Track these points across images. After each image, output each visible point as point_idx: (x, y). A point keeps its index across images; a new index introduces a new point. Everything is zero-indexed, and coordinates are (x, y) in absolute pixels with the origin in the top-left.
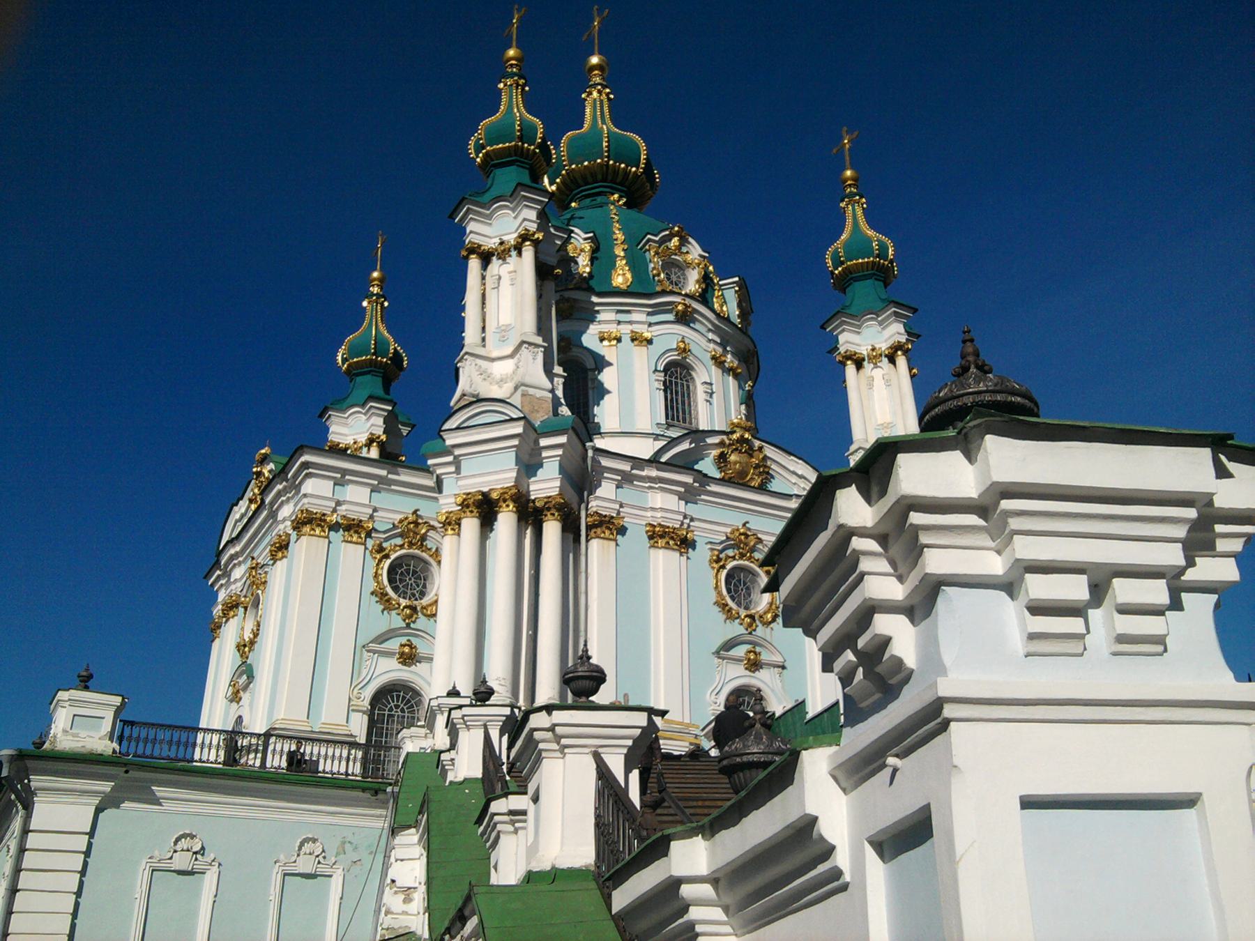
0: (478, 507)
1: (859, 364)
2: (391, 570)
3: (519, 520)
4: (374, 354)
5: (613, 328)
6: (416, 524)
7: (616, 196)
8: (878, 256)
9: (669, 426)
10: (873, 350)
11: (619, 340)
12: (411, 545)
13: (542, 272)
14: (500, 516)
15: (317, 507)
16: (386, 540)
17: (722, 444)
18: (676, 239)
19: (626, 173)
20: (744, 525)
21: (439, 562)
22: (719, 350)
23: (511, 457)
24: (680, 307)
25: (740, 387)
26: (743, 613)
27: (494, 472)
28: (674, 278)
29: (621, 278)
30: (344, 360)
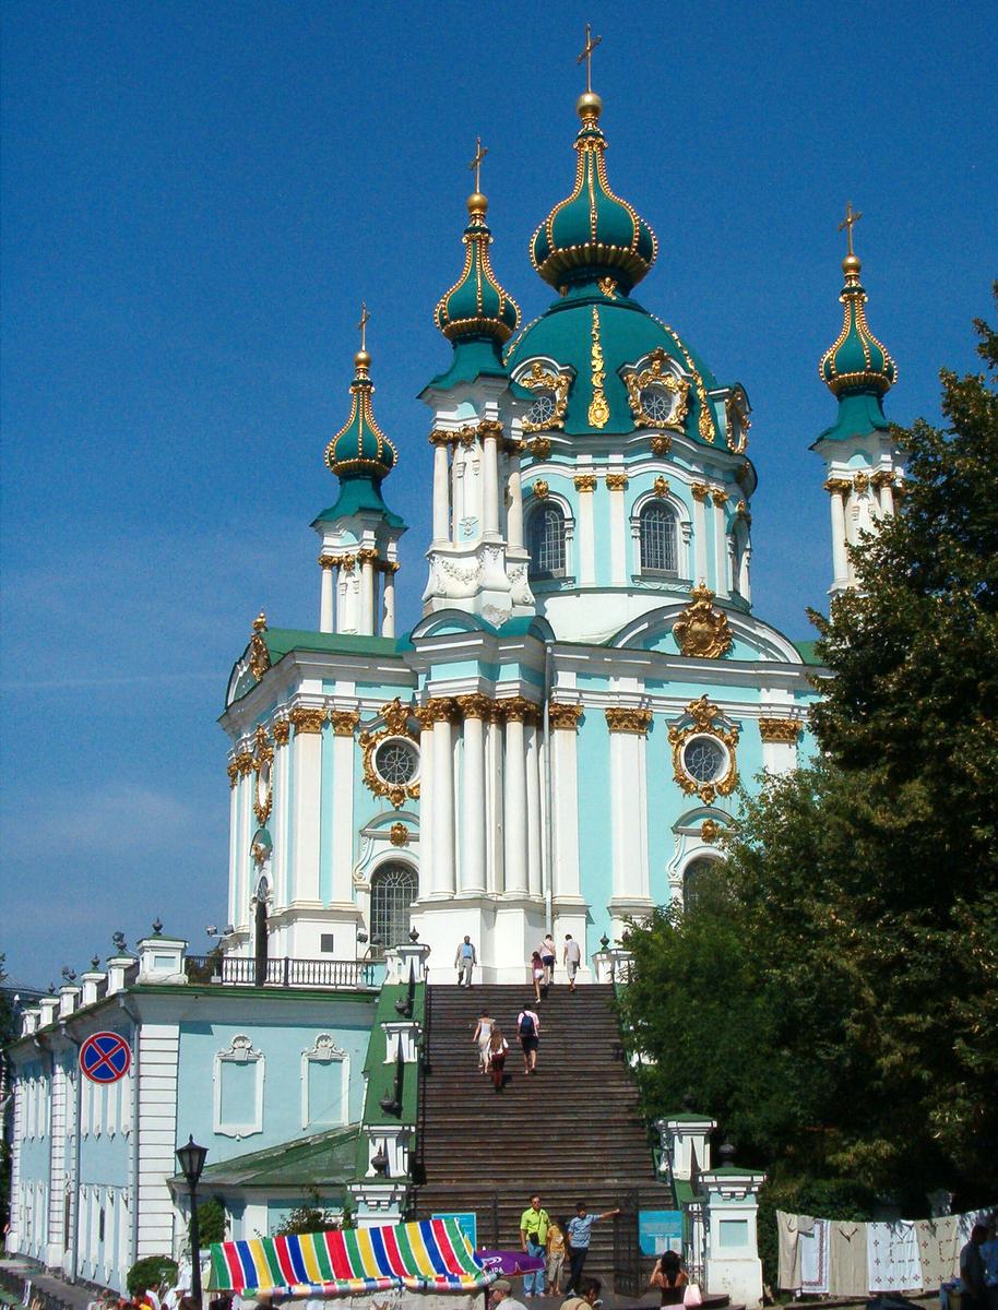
0: (446, 712)
1: (845, 492)
2: (380, 756)
4: (363, 457)
5: (588, 472)
7: (608, 279)
8: (869, 370)
9: (644, 577)
10: (859, 477)
11: (594, 485)
13: (508, 449)
14: (467, 722)
15: (308, 704)
16: (371, 730)
17: (682, 618)
19: (618, 254)
20: (704, 697)
21: (419, 743)
22: (701, 482)
24: (659, 442)
25: (726, 512)
26: (702, 785)
29: (599, 415)
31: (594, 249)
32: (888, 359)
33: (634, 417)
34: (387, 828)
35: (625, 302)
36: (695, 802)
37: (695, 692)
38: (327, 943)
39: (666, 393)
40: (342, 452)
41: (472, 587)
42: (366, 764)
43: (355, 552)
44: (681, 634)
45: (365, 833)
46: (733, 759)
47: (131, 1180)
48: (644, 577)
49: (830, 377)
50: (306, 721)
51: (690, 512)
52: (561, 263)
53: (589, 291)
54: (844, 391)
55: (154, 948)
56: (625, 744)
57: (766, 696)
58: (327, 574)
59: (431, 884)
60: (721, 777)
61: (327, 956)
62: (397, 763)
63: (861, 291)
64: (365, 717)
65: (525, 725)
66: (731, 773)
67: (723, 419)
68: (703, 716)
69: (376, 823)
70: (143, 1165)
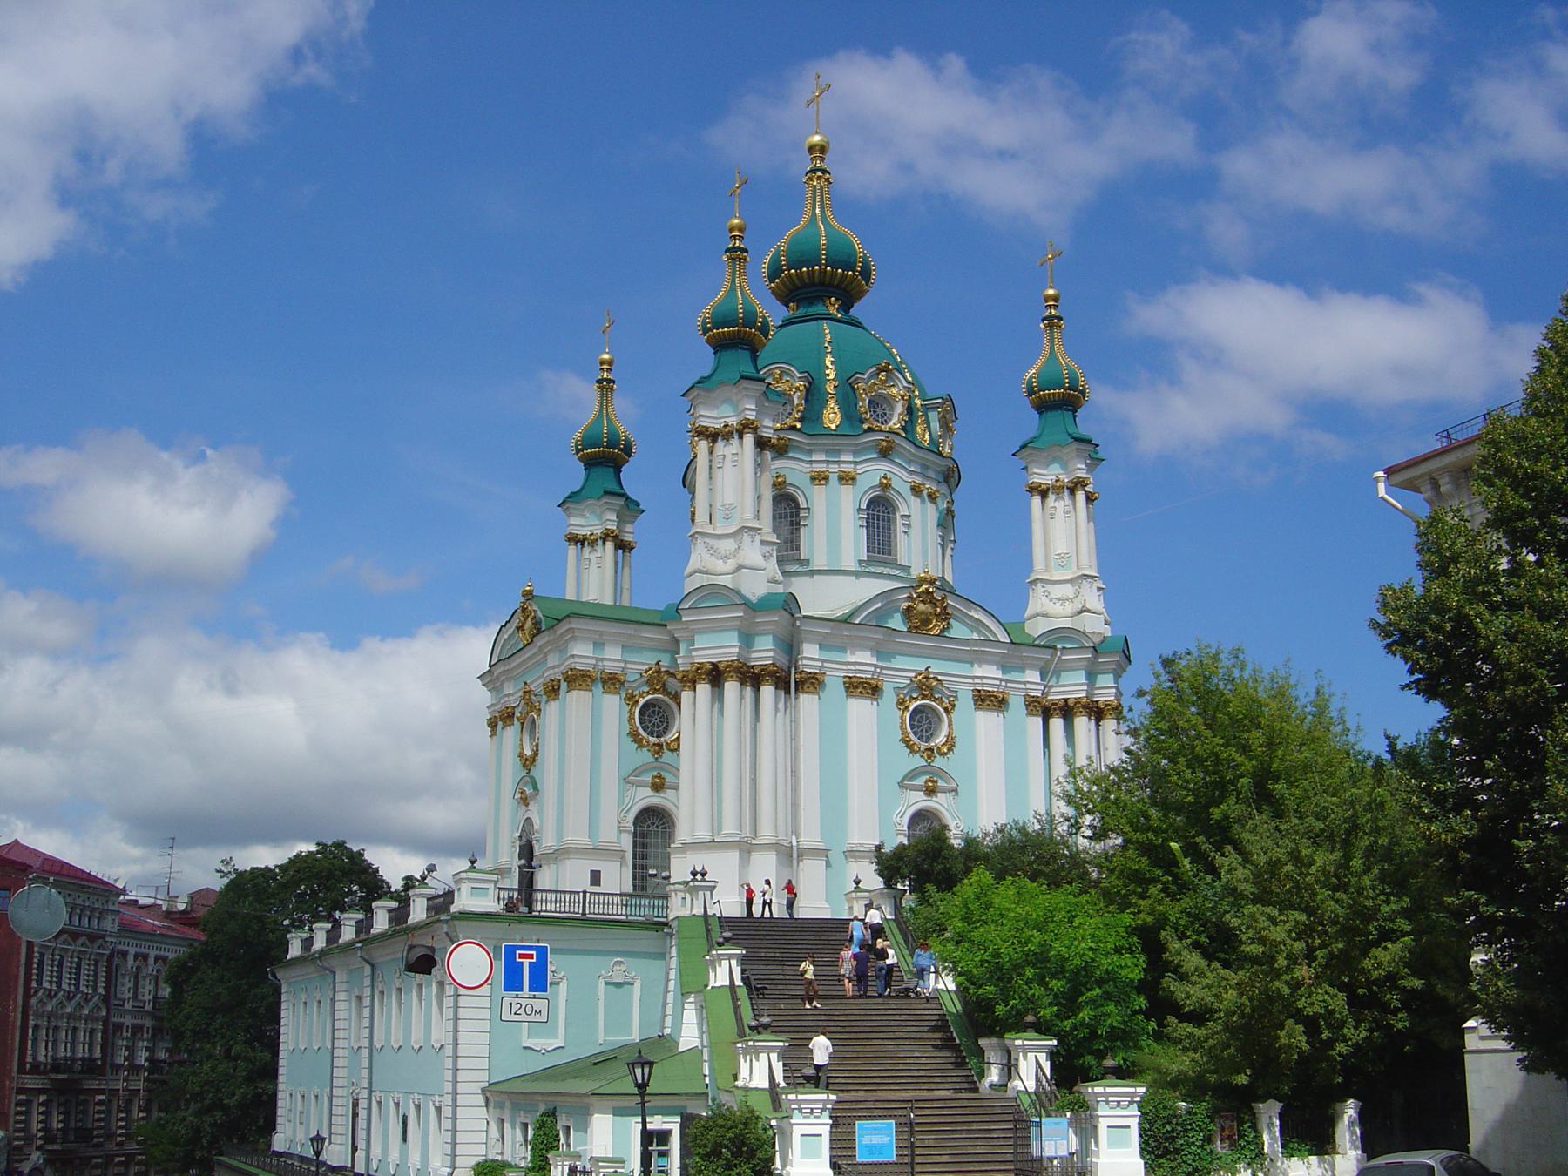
1: (1044, 494)
2: (641, 713)
5: (822, 468)
6: (658, 672)
9: (869, 562)
11: (826, 478)
12: (656, 691)
13: (761, 444)
15: (583, 664)
17: (910, 598)
18: (882, 376)
19: (844, 276)
21: (679, 705)
23: (736, 634)
26: (924, 746)
28: (879, 411)
29: (832, 417)
30: (578, 451)
32: (1082, 381)
34: (648, 778)
35: (846, 318)
36: (917, 761)
37: (919, 665)
38: (596, 878)
39: (889, 401)
41: (731, 564)
42: (631, 719)
43: (598, 531)
46: (950, 725)
47: (449, 1087)
48: (869, 562)
49: (1031, 392)
52: (792, 282)
53: (818, 309)
54: (1043, 406)
55: (471, 880)
56: (859, 708)
57: (978, 671)
58: (572, 550)
60: (940, 739)
61: (595, 889)
63: (1060, 319)
64: (631, 678)
67: (935, 426)
68: (925, 685)
69: (637, 772)
70: (461, 1076)
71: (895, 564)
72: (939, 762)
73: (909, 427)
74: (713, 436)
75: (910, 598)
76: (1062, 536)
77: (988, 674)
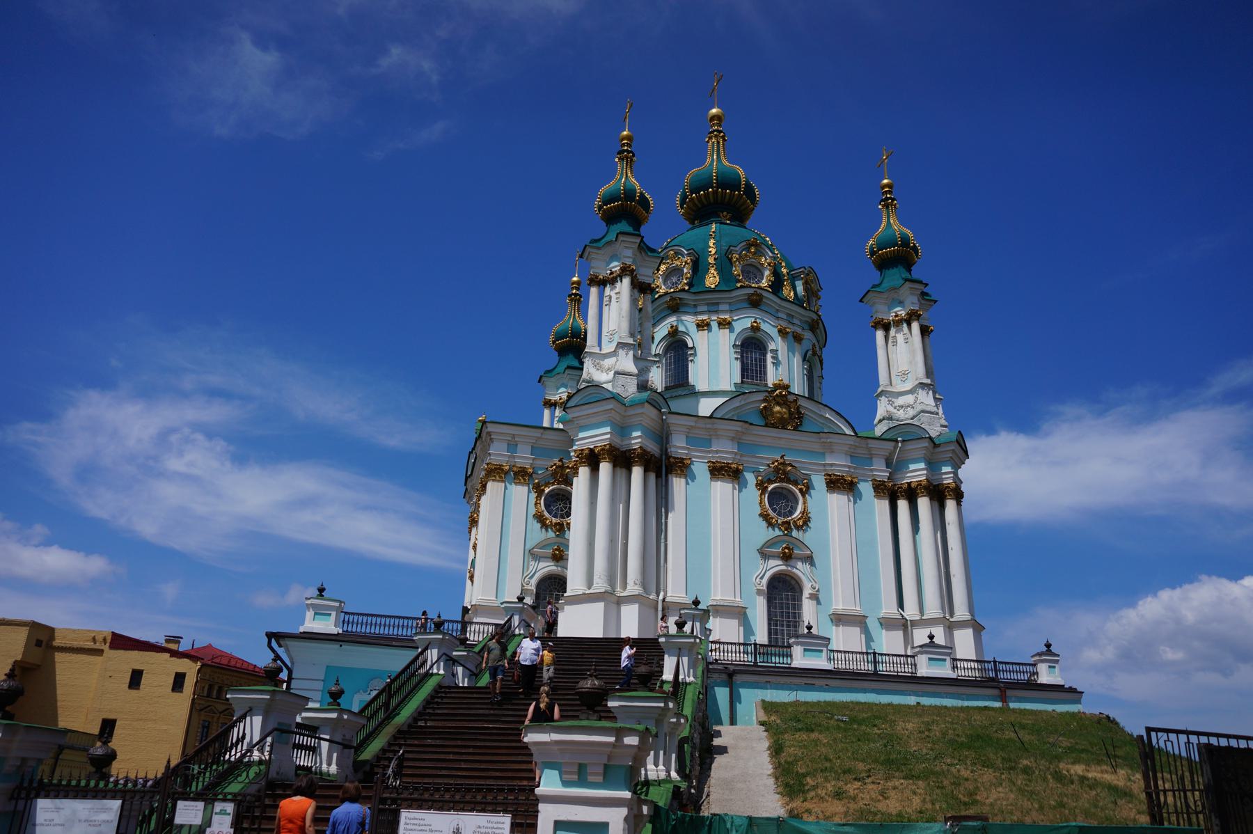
1: (886, 328)
3: (614, 466)
6: (562, 467)
8: (902, 245)
11: (708, 325)
13: (641, 288)
17: (765, 400)
22: (784, 324)
27: (596, 436)
29: (712, 280)
31: (715, 193)
33: (739, 281)
40: (559, 336)
44: (765, 413)
45: (533, 554)
46: (805, 503)
49: (873, 253)
50: (496, 472)
51: (777, 344)
52: (695, 204)
56: (722, 490)
59: (575, 585)
60: (797, 514)
62: (560, 505)
63: (893, 200)
65: (646, 471)
66: (804, 512)
71: (766, 385)
72: (795, 533)
73: (777, 286)
74: (602, 283)
75: (765, 400)
76: (902, 357)
77: (840, 463)
